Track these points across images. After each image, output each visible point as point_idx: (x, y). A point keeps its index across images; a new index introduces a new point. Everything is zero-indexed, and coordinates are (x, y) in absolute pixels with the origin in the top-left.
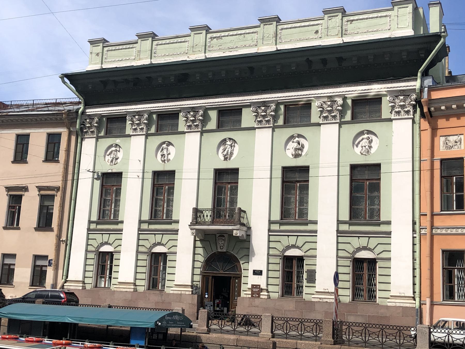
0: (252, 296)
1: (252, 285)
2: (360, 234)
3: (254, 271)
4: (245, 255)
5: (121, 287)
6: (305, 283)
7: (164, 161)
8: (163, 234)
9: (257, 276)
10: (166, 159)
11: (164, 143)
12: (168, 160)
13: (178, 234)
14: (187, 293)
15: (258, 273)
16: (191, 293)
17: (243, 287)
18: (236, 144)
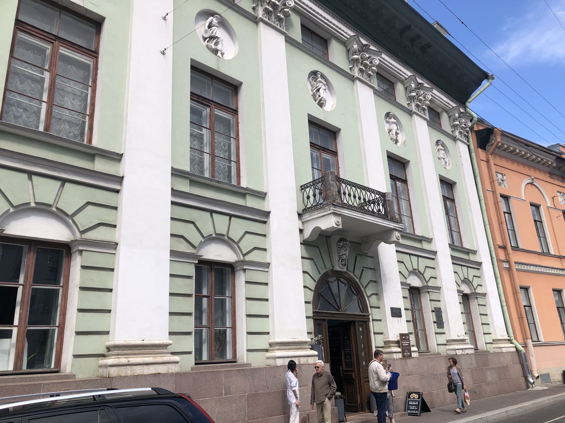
1: (401, 335)
2: (462, 262)
5: (133, 360)
6: (431, 328)
7: (215, 52)
8: (231, 216)
9: (396, 318)
11: (212, 14)
15: (396, 313)
18: (327, 90)
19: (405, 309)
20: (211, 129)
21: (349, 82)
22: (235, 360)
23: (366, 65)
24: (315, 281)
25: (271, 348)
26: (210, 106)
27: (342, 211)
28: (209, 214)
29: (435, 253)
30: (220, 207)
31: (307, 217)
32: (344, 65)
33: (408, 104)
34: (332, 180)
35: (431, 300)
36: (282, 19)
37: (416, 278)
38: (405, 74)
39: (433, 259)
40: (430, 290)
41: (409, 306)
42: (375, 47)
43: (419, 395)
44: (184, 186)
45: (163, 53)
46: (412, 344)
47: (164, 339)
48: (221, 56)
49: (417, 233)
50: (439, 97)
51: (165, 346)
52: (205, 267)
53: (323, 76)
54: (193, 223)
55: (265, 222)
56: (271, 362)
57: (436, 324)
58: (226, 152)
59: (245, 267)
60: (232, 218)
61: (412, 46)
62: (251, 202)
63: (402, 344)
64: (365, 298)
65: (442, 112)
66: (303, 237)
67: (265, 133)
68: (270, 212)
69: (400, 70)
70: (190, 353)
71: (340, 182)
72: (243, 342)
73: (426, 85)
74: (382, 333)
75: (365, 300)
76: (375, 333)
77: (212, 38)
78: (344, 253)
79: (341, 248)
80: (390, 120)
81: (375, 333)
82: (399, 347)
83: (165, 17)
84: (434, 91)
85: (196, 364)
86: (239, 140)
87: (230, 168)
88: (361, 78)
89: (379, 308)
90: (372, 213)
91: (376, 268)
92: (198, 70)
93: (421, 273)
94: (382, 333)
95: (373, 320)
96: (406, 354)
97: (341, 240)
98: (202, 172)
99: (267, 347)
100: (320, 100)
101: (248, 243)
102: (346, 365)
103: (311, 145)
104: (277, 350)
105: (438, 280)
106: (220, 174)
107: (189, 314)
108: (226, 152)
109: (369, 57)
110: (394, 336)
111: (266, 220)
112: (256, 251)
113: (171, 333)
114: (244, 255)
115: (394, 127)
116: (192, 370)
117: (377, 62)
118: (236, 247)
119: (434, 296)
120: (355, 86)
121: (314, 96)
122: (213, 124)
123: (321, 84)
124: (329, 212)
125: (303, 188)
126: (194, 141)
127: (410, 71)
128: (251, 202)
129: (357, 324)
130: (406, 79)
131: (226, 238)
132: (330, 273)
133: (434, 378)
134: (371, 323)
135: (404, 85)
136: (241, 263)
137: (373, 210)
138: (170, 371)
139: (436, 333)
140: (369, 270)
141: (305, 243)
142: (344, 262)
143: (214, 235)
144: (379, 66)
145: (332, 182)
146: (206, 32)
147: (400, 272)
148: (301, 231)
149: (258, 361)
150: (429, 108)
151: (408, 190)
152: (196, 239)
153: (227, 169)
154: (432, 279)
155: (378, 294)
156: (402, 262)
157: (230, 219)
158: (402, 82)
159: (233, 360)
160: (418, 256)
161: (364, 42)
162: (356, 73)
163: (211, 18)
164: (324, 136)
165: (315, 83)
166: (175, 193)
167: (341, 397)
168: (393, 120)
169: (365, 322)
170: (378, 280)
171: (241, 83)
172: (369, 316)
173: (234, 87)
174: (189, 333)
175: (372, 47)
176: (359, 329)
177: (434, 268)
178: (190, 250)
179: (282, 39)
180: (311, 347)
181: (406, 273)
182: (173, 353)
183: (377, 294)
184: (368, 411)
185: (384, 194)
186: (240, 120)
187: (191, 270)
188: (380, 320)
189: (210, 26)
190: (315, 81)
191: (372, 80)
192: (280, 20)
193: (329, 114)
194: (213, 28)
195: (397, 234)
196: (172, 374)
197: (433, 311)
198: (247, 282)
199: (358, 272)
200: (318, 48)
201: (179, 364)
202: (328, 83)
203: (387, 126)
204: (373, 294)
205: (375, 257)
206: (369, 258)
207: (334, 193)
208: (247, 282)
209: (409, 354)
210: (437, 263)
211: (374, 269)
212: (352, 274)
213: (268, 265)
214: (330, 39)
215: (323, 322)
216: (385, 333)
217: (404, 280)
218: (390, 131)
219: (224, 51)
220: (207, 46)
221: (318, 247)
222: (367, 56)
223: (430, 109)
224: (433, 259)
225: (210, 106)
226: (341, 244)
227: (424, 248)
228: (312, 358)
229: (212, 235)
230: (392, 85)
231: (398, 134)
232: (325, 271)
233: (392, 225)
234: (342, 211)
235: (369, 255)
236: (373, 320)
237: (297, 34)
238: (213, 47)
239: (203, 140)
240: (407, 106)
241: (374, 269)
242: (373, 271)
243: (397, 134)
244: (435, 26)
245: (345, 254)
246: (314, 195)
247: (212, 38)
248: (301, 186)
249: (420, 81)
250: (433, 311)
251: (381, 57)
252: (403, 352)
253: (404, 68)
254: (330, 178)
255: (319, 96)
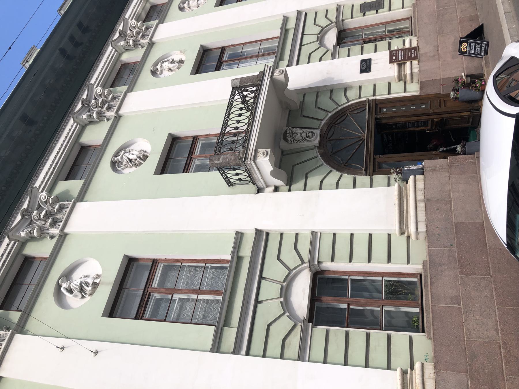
0: (415, 58)
1: (391, 61)
3: (362, 71)
4: (331, 98)
7: (95, 285)
8: (261, 278)
10: (90, 281)
12: (98, 276)
13: (268, 234)
14: (420, 185)
15: (366, 66)
16: (420, 177)
17: (398, 92)
18: (131, 148)
19: (362, 54)
20: (173, 291)
21: (122, 122)
22: (419, 276)
23: (104, 103)
24: (331, 172)
25: (406, 233)
26: (150, 293)
27: (251, 148)
28: (259, 305)
29: (299, 13)
30: (245, 328)
31: (260, 184)
32: (106, 126)
33: (142, 47)
34: (219, 160)
35: (352, 18)
36: (60, 206)
37: (327, 37)
38: (111, 52)
39: (306, 14)
40: (341, 20)
41: (358, 48)
42: (84, 92)
43: (463, 41)
44: (230, 335)
45: (96, 353)
46: (401, 47)
47: (395, 376)
48: (99, 280)
49: (278, 34)
50: (134, 8)
51: (404, 373)
52: (317, 305)
53: (116, 155)
54: (269, 326)
55: (268, 234)
56: (422, 237)
57: (379, 11)
58: (196, 271)
59: (316, 263)
60: (263, 276)
61: (81, 44)
62: (246, 251)
63: (402, 60)
64: (349, 106)
65: (150, 3)
66: (283, 186)
67: (175, 231)
68: (256, 230)
69: (108, 58)
70: (411, 338)
71: (224, 134)
72: (399, 266)
73: (121, 28)
74: (390, 84)
75: (352, 105)
76: (389, 93)
77: (81, 290)
78: (299, 135)
79: (294, 139)
80: (159, 69)
81: (389, 93)
82: (405, 64)
83: (61, 348)
84: (127, 16)
85: (423, 332)
86: (183, 260)
87: (212, 268)
88: (116, 108)
89: (360, 87)
90: (256, 98)
91: (317, 91)
92: (112, 311)
93: (322, 30)
94: (390, 84)
95: (374, 95)
96: (413, 55)
97: (285, 138)
98: (218, 301)
99: (404, 238)
100: (140, 158)
101: (290, 258)
102: (424, 126)
103: (186, 172)
104: (408, 228)
105: (328, 8)
106: (219, 278)
107: (368, 336)
108: (196, 271)
109: (95, 99)
110: (393, 70)
111: (265, 233)
112: (299, 247)
113: (389, 368)
114: (303, 262)
115: (166, 65)
116: (430, 339)
117: (99, 89)
118: (294, 271)
119: (347, 13)
120: (125, 115)
121: (136, 165)
122: (167, 289)
123: (124, 157)
124: (253, 164)
125: (230, 184)
126: (186, 308)
127: (107, 48)
128: (246, 251)
129: (379, 116)
130: (116, 51)
131: (285, 284)
132: (322, 151)
133: (443, 15)
134: (378, 98)
135: (123, 53)
136: (312, 267)
137: (252, 98)
138: (433, 375)
139: (390, 10)
140: (319, 100)
141: (290, 183)
142: (310, 134)
143: (282, 299)
144: (104, 87)
145: (221, 161)
146: (76, 296)
147: (320, 60)
148: (276, 189)
149: (420, 252)
150: (144, 22)
151: (232, 45)
152: (286, 323)
153: (214, 270)
154: (328, 16)
155: (346, 89)
156: (310, 55)
157: (265, 278)
158: (120, 55)
159: (419, 278)
160: (303, 34)
161: (19, 217)
162: (111, 114)
163: (62, 289)
164: (178, 155)
165: (124, 163)
166: (236, 351)
167: (463, 147)
168: (158, 67)
169: (376, 104)
170: (330, 89)
171: (125, 256)
172: (369, 100)
173: (130, 263)
174: (389, 338)
175: (25, 206)
176: (385, 113)
177: (316, 13)
178: (298, 331)
179: (80, 206)
180: (405, 183)
181: (322, 50)
182: (412, 367)
183: (346, 90)
184: (479, 103)
185: (233, 88)
186: (163, 258)
187: (320, 330)
188: (375, 85)
189: (70, 291)
190: (122, 163)
191: (118, 94)
192: (61, 208)
193: (154, 147)
194: (72, 287)
195: (276, 74)
196: (436, 374)
197: (364, 15)
198: (333, 260)
199: (321, 115)
200: (89, 159)
201: (425, 363)
202: (124, 148)
203: (166, 73)
204: (345, 95)
205: (304, 92)
206: (305, 100)
207: (233, 157)
208: (333, 260)
209: (413, 51)
210: (310, 10)
211: (318, 93)
212: (323, 122)
213: (314, 234)
214: (23, 255)
215: (377, 160)
216: (389, 80)
217: (329, 54)
218: (170, 70)
219: (93, 275)
220: (91, 294)
221: (293, 166)
222: (93, 101)
223: (148, 17)
224: (306, 14)
225: (150, 293)
226: (289, 139)
227: (294, 26)
228: (417, 183)
229: (281, 302)
230: (125, 66)
231: (173, 60)
232: (320, 157)
233: (267, 81)
234: (251, 152)
235: (302, 100)
236: (374, 95)
237: (74, 186)
238: (90, 288)
239: (184, 299)
240: (145, 49)
241: (318, 93)
242: (319, 95)
243: (173, 62)
244: (63, 12)
245: (301, 134)
246: (237, 174)
247: (81, 290)
248: (229, 186)
249: (117, 35)
250: (364, 15)
251: (40, 187)
252: (411, 59)
253: (105, 53)
254: (216, 162)
255: (136, 160)
